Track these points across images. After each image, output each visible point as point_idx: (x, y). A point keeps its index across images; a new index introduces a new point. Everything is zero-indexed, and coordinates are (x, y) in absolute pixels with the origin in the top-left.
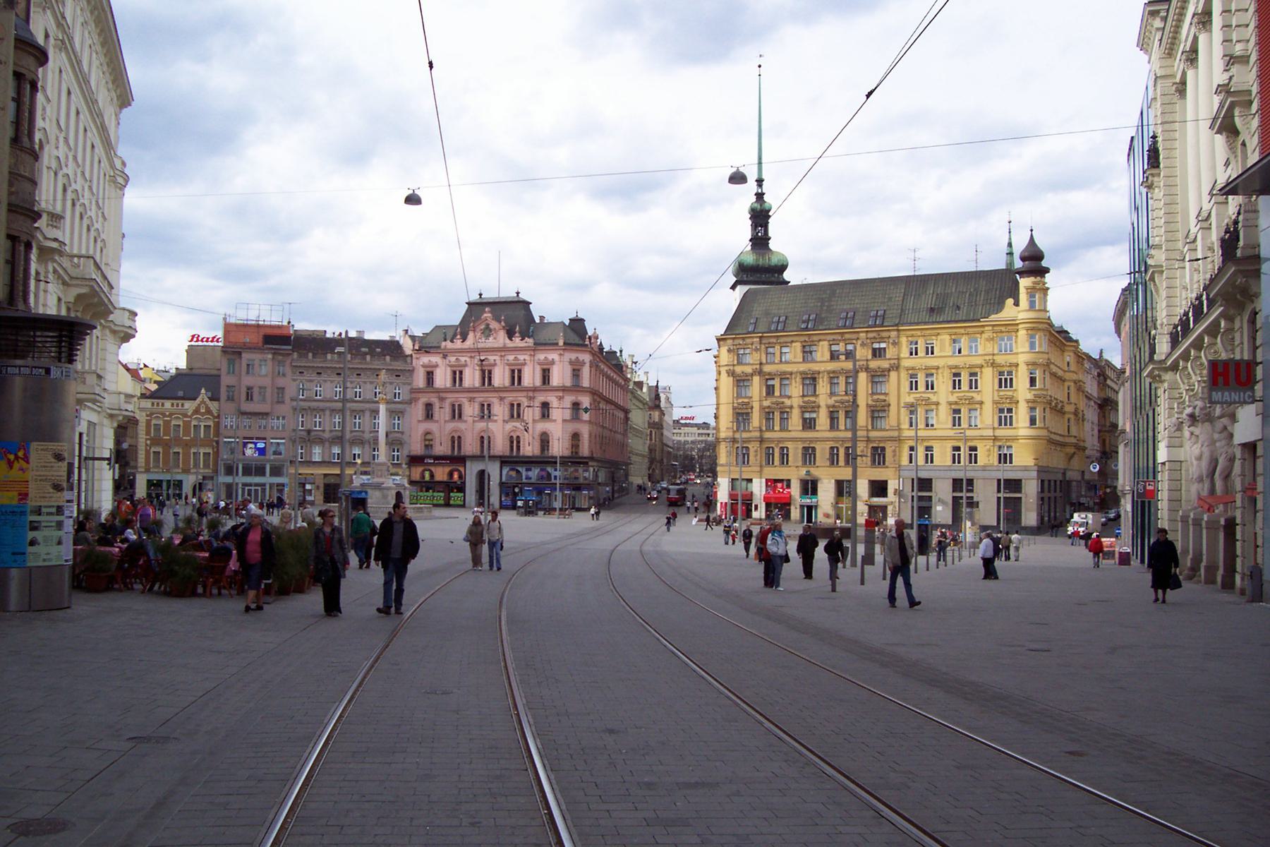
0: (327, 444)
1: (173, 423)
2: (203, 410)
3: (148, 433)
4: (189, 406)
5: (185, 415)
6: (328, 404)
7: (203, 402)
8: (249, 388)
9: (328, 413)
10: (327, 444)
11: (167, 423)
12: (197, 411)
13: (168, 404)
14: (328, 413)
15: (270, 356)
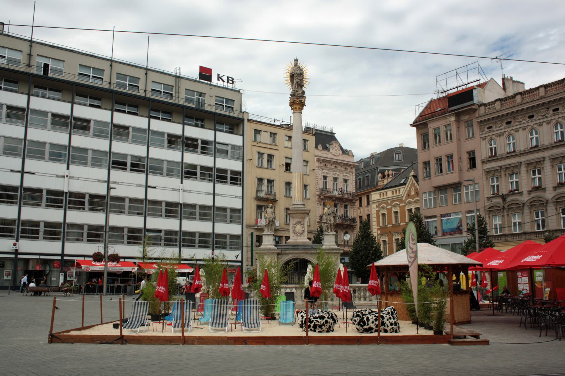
0: (526, 211)
1: (394, 210)
2: (413, 193)
3: (378, 224)
4: (403, 190)
5: (401, 201)
6: (523, 159)
7: (413, 185)
8: (439, 160)
9: (523, 169)
10: (526, 211)
11: (389, 210)
12: (409, 195)
13: (389, 193)
14: (523, 169)
15: (453, 119)
